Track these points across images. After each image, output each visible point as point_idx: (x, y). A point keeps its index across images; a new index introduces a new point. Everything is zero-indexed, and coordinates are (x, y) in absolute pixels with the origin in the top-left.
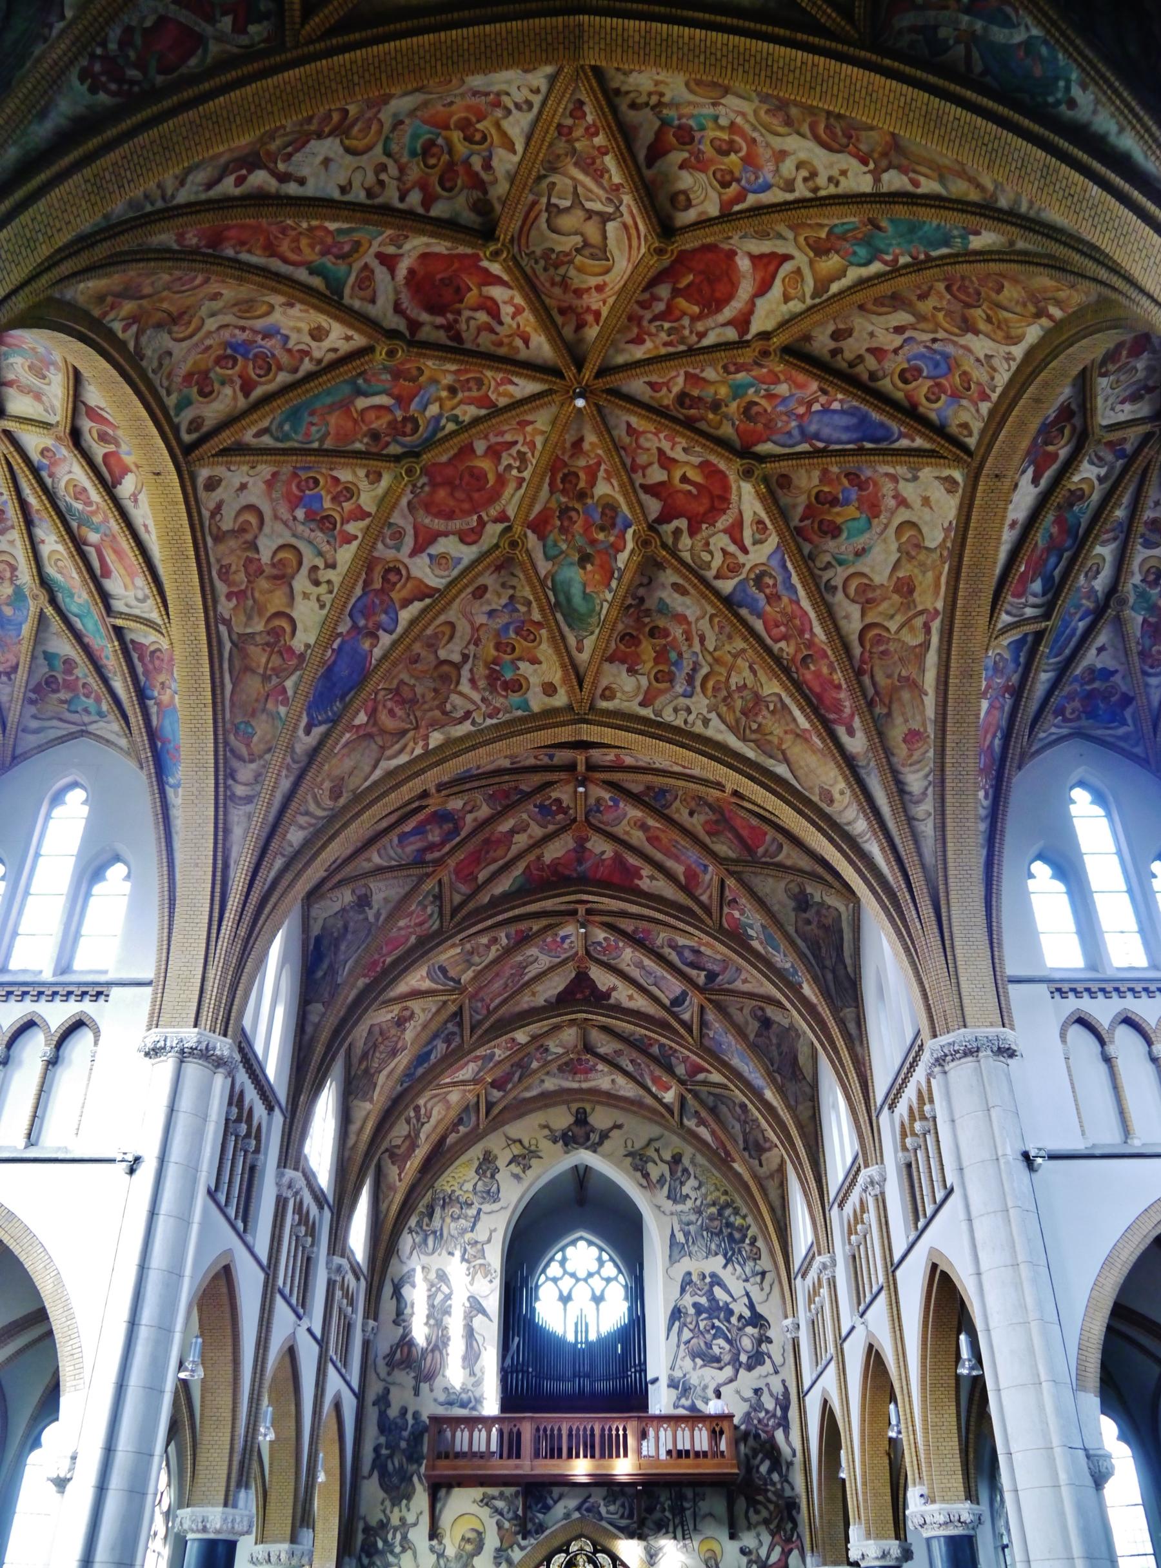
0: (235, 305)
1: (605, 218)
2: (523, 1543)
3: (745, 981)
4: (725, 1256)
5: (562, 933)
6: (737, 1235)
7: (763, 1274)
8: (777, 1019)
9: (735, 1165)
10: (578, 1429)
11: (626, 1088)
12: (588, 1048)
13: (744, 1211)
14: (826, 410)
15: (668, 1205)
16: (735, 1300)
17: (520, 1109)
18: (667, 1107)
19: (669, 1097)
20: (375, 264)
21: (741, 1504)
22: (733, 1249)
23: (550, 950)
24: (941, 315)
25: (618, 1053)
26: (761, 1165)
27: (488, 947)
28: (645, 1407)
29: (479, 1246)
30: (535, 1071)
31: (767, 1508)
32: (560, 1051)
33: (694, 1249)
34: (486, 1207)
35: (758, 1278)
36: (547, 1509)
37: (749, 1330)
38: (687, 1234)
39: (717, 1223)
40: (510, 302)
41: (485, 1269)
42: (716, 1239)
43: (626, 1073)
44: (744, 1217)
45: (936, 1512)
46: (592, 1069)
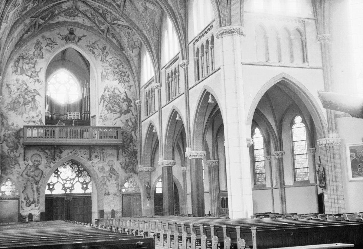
2: (54, 162)
4: (119, 80)
6: (123, 74)
7: (131, 86)
8: (150, 7)
9: (124, 52)
10: (73, 130)
11: (88, 23)
12: (77, 9)
13: (126, 67)
15: (101, 63)
16: (121, 94)
17: (51, 27)
18: (103, 31)
21: (121, 151)
22: (121, 78)
25: (87, 11)
26: (133, 53)
28: (90, 124)
29: (36, 73)
30: (57, 15)
31: (128, 152)
32: (66, 8)
33: (109, 77)
34: (38, 60)
35: (129, 88)
36: (61, 152)
37: (126, 103)
38: (107, 73)
39: (117, 70)
41: (39, 81)
42: (116, 75)
43: (89, 18)
44: (125, 69)
45: (194, 153)
46: (77, 15)
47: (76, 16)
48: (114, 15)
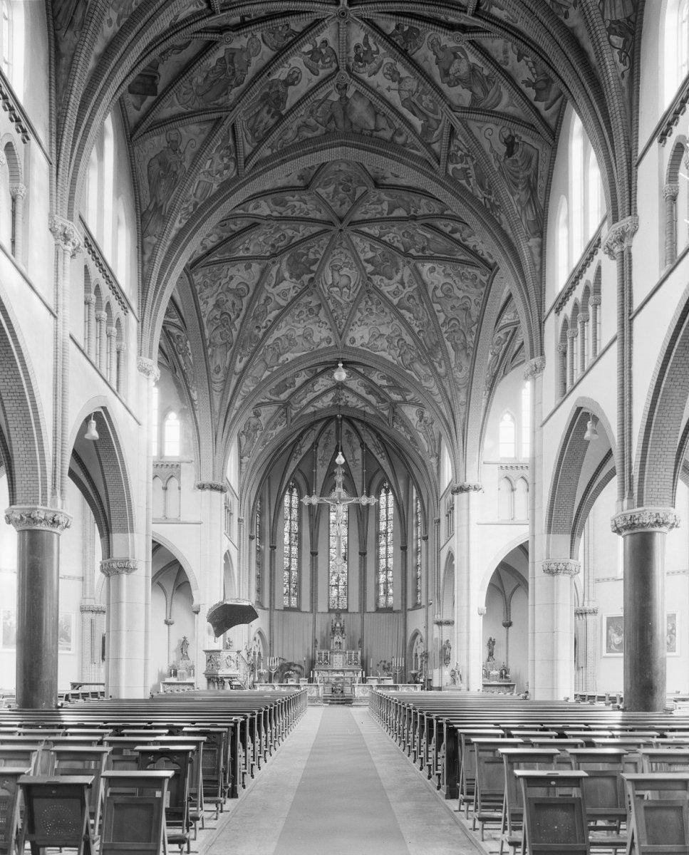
0: (451, 297)
1: (333, 285)
14: (244, 243)
20: (406, 285)
24: (225, 299)
40: (365, 252)
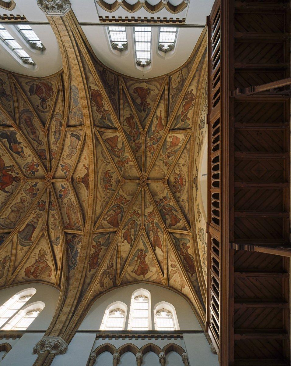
3: (59, 110)
5: (61, 188)
19: (180, 136)
23: (67, 193)
27: (55, 218)
46: (179, 175)
47: (180, 177)
48: (156, 128)
